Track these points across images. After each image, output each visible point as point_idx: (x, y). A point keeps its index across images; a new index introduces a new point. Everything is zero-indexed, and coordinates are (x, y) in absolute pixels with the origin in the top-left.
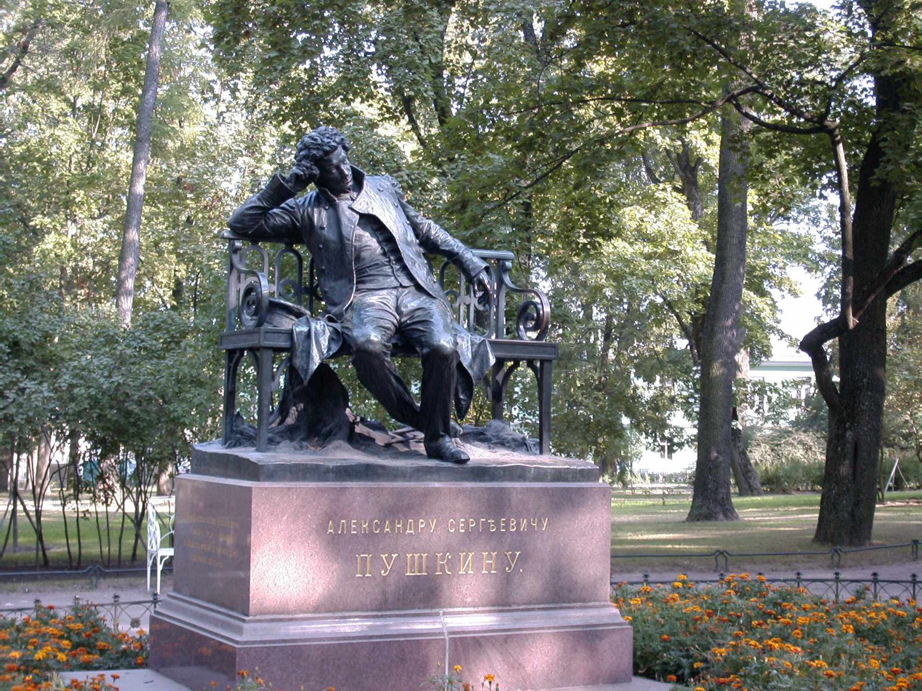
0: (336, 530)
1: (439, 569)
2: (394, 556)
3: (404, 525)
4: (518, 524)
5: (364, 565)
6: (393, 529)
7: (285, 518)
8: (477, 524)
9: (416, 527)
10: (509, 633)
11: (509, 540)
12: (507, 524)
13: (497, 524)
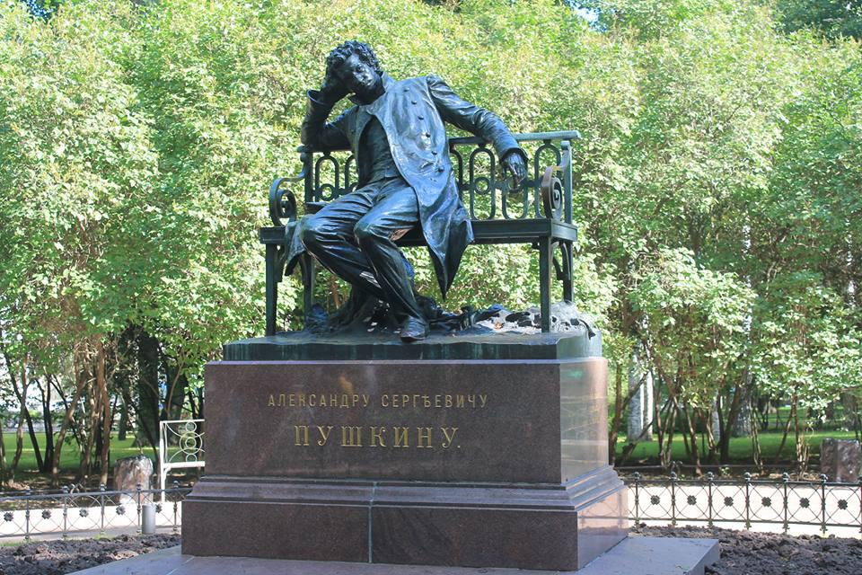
0: (276, 402)
1: (373, 442)
3: (339, 399)
4: (454, 401)
5: (302, 434)
6: (328, 403)
7: (232, 391)
10: (435, 507)
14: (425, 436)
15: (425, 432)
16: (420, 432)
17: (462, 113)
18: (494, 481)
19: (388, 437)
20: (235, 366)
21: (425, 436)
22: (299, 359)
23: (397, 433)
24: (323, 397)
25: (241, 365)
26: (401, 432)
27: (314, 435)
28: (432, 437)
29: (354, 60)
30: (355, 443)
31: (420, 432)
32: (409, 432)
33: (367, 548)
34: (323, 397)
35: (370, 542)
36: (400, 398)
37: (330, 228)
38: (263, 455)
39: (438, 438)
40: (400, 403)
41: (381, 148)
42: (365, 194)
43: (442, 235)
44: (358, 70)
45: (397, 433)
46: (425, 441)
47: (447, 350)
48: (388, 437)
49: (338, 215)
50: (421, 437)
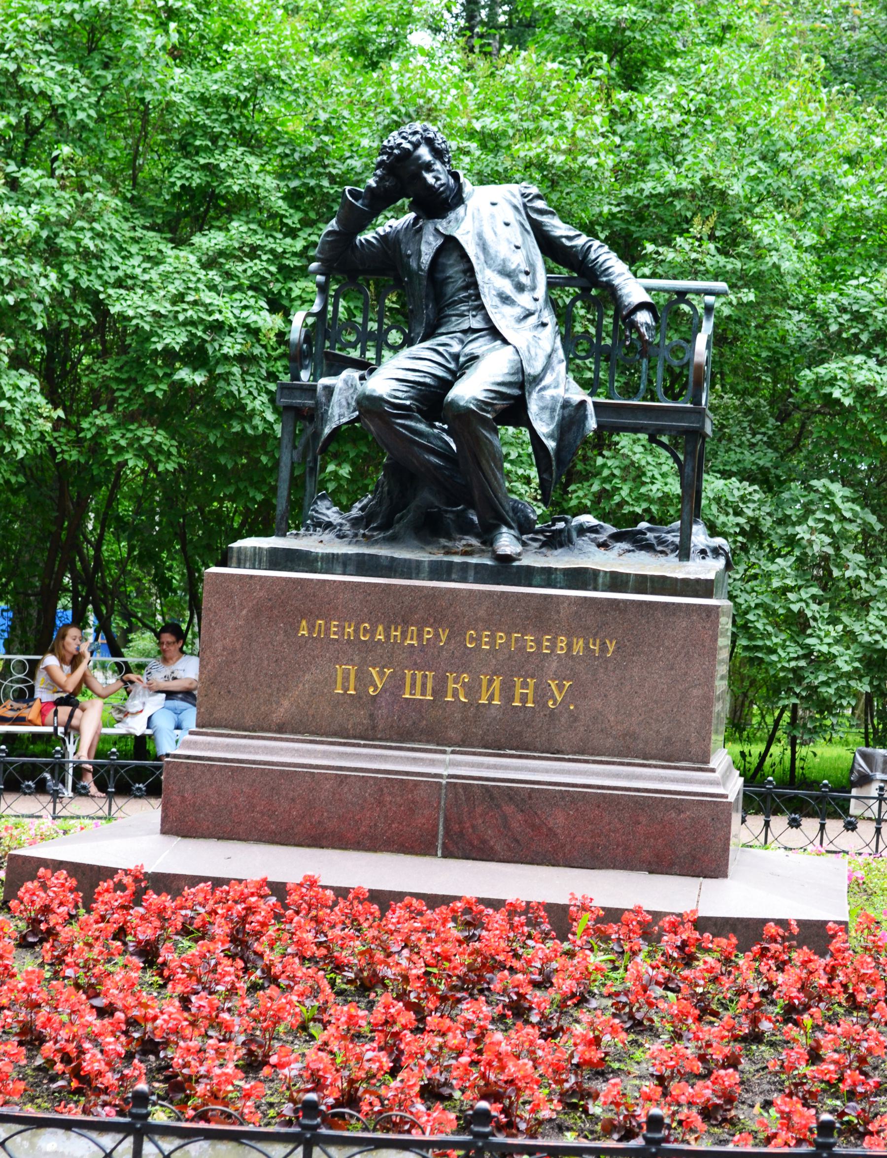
1: (450, 693)
2: (388, 672)
3: (404, 634)
4: (570, 646)
5: (346, 679)
6: (388, 637)
8: (509, 639)
9: (420, 637)
11: (555, 664)
12: (554, 642)
13: (538, 643)
14: (525, 691)
15: (525, 685)
16: (518, 685)
17: (568, 243)
18: (619, 755)
19: (472, 690)
20: (251, 577)
21: (525, 691)
22: (344, 574)
23: (485, 683)
24: (380, 628)
25: (261, 577)
26: (491, 681)
27: (363, 679)
28: (535, 692)
29: (424, 153)
30: (423, 693)
31: (518, 685)
32: (503, 683)
33: (435, 836)
34: (380, 628)
35: (441, 828)
36: (493, 637)
37: (399, 394)
38: (286, 703)
39: (542, 694)
40: (493, 642)
41: (460, 283)
42: (441, 349)
43: (552, 418)
44: (428, 167)
45: (485, 683)
46: (524, 698)
47: (560, 577)
48: (472, 690)
49: (411, 376)
50: (519, 691)
